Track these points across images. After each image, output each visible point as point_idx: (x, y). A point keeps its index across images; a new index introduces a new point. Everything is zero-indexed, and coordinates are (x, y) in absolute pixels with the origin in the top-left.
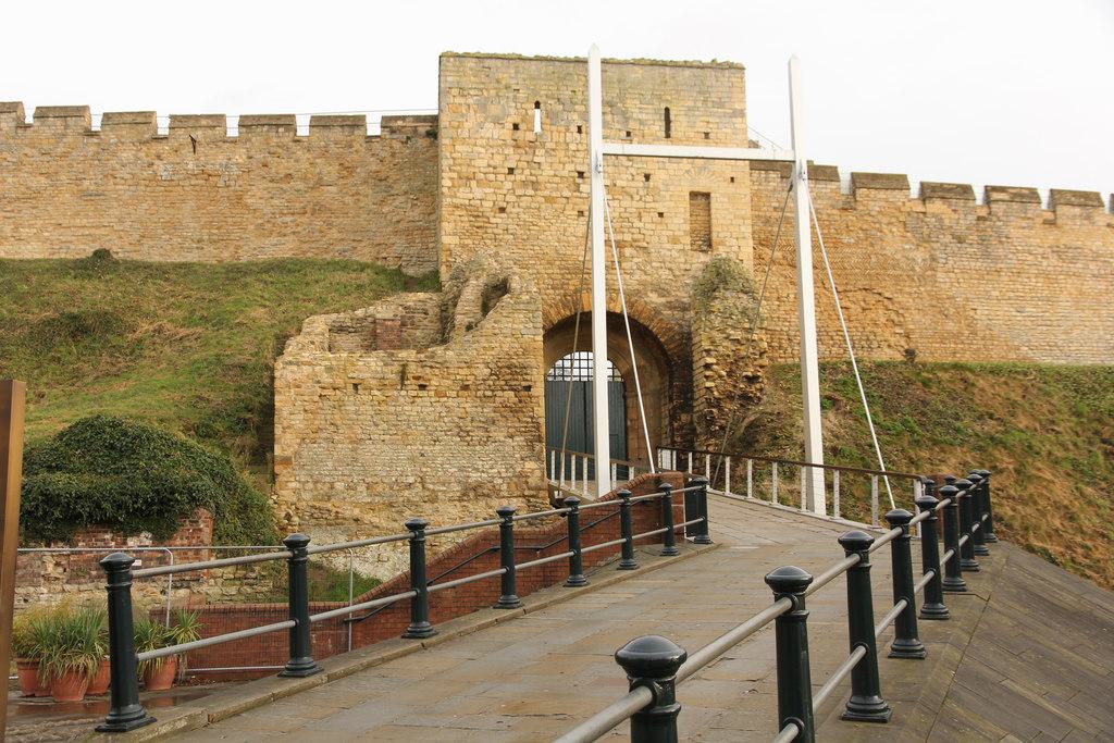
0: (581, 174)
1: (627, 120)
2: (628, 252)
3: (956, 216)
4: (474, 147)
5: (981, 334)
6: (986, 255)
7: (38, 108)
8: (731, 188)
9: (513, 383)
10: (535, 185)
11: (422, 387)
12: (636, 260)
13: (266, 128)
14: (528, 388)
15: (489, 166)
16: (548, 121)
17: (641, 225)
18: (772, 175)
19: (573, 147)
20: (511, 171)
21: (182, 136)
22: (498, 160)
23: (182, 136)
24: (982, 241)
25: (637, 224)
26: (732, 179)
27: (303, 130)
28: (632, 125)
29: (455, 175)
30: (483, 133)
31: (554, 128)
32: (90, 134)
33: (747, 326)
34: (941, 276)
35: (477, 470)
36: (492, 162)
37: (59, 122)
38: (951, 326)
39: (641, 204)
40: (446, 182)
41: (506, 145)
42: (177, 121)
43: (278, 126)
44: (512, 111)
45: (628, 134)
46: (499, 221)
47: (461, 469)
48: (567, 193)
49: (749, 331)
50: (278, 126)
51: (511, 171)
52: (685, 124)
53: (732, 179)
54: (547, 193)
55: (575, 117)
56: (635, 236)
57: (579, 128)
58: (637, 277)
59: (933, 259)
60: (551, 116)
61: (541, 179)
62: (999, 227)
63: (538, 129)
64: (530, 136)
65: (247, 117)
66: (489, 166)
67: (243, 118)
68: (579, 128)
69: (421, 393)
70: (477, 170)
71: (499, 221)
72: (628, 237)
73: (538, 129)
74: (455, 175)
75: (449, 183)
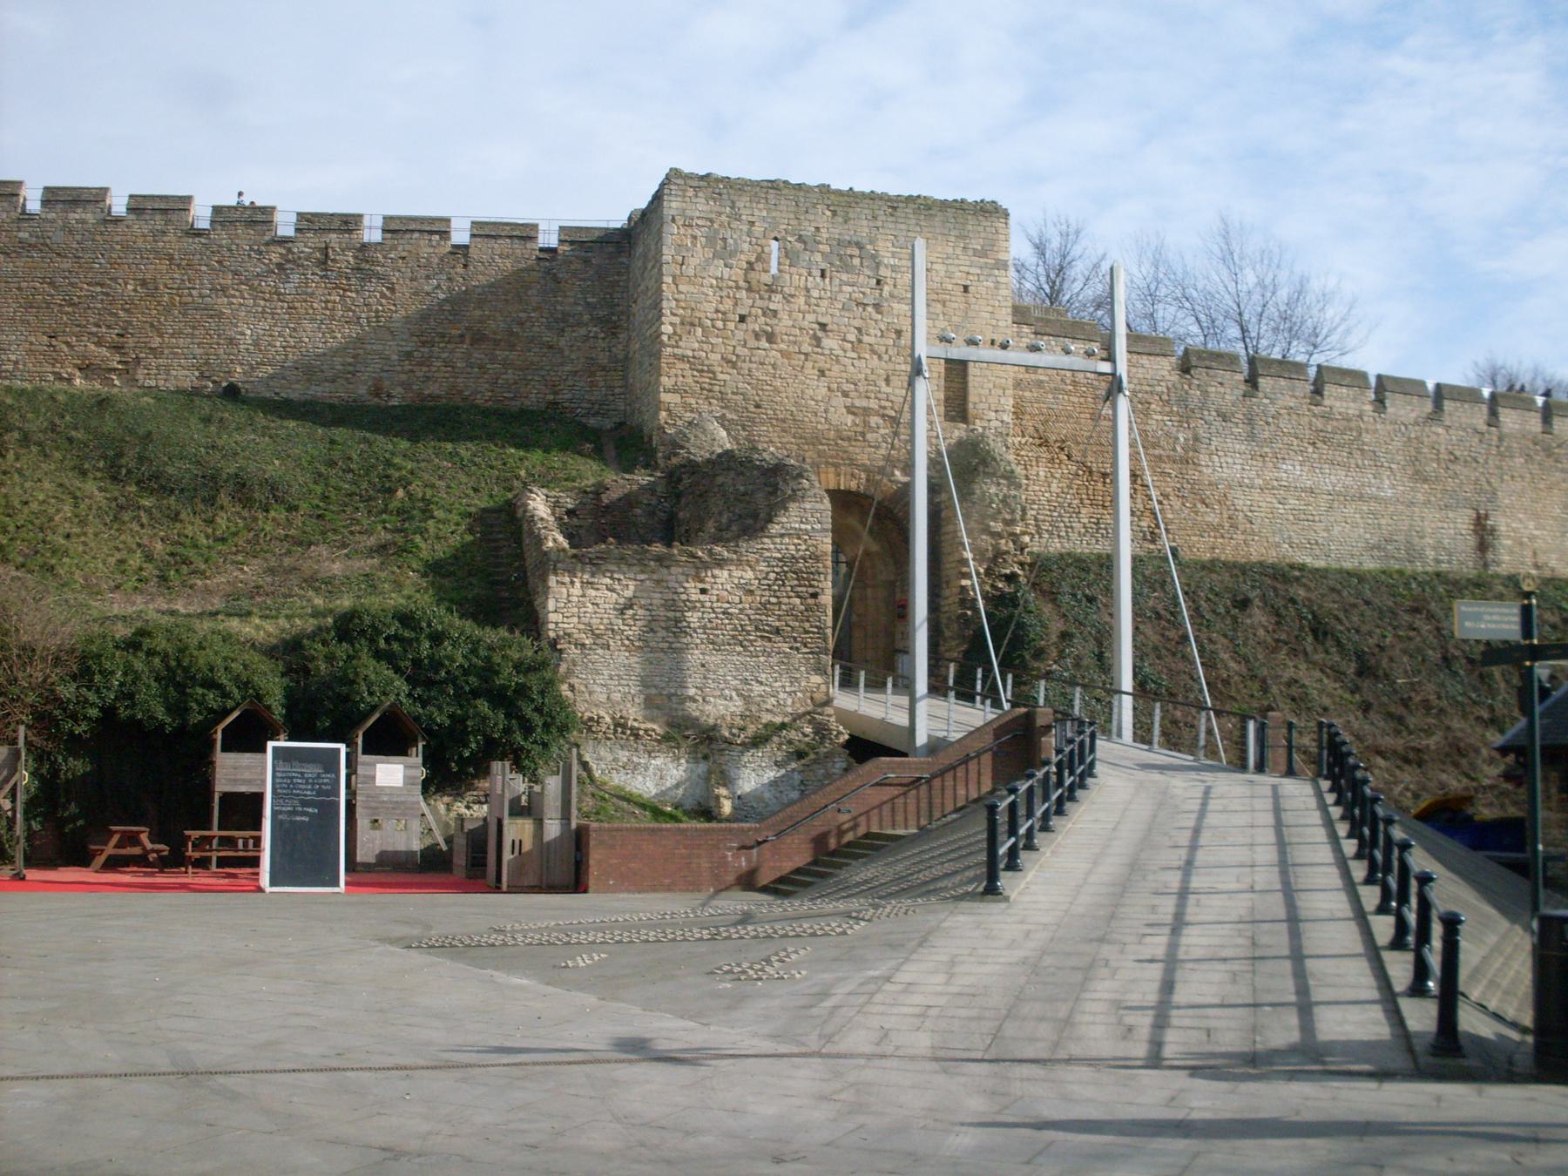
0: (823, 326)
1: (878, 265)
3: (1222, 390)
4: (689, 280)
5: (1241, 527)
6: (1251, 437)
7: (131, 196)
10: (771, 338)
11: (703, 591)
12: (882, 431)
13: (416, 235)
14: (815, 596)
15: (717, 311)
17: (889, 390)
18: (1026, 329)
19: (815, 294)
20: (742, 319)
21: (313, 240)
22: (727, 305)
24: (1250, 421)
25: (885, 389)
27: (460, 236)
28: (883, 272)
29: (677, 320)
30: (712, 270)
31: (793, 270)
33: (1008, 517)
34: (1203, 459)
35: (761, 683)
36: (721, 307)
37: (158, 217)
38: (1212, 518)
39: (891, 366)
41: (738, 288)
42: (308, 222)
43: (431, 232)
44: (746, 246)
45: (878, 282)
46: (727, 377)
47: (745, 681)
48: (806, 348)
49: (1007, 523)
50: (431, 232)
51: (742, 319)
52: (942, 274)
54: (783, 346)
55: (818, 257)
56: (884, 403)
59: (1196, 439)
60: (787, 253)
61: (777, 329)
62: (1266, 405)
63: (774, 271)
64: (766, 278)
66: (717, 311)
67: (388, 219)
69: (702, 597)
70: (702, 315)
71: (727, 377)
72: (873, 404)
73: (774, 271)
74: (677, 320)
75: (670, 330)
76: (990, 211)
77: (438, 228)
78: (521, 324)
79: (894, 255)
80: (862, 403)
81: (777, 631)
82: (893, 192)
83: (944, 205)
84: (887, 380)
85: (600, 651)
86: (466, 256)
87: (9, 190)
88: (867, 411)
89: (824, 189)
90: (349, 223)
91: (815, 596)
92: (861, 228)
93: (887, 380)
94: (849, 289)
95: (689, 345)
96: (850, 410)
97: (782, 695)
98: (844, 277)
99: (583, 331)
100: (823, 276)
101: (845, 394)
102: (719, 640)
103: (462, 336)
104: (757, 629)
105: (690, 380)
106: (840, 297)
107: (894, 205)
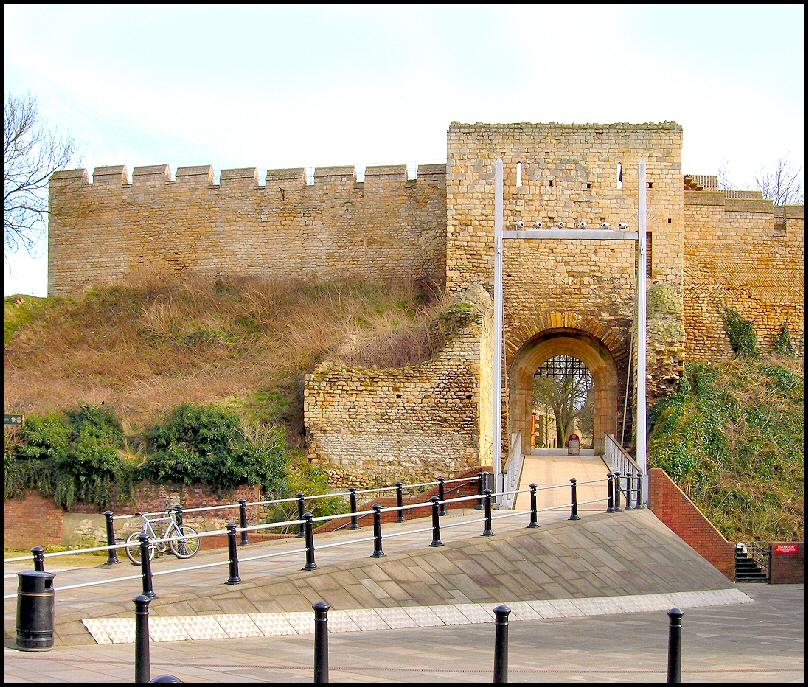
1: (588, 175)
2: (586, 280)
8: (669, 228)
9: (460, 393)
11: (399, 396)
12: (592, 287)
14: (469, 397)
16: (527, 177)
21: (276, 186)
23: (273, 192)
25: (594, 258)
26: (670, 221)
30: (478, 188)
32: (213, 187)
37: (192, 179)
40: (450, 229)
42: (273, 175)
45: (589, 186)
49: (671, 344)
53: (670, 221)
56: (593, 268)
57: (551, 182)
58: (593, 301)
60: (528, 174)
63: (519, 184)
65: (320, 169)
68: (551, 182)
69: (399, 400)
72: (586, 269)
73: (519, 184)
76: (670, 128)
77: (347, 173)
78: (396, 231)
79: (599, 166)
80: (581, 269)
81: (445, 420)
82: (601, 123)
83: (636, 128)
84: (595, 252)
85: (336, 435)
86: (362, 189)
87: (116, 171)
88: (582, 274)
89: (553, 126)
90: (294, 174)
91: (469, 397)
92: (577, 149)
93: (595, 252)
94: (569, 192)
95: (464, 238)
96: (571, 274)
97: (448, 460)
98: (565, 184)
99: (432, 233)
100: (551, 184)
101: (567, 263)
102: (407, 427)
103: (362, 241)
104: (432, 419)
105: (466, 262)
106: (563, 198)
107: (599, 131)
